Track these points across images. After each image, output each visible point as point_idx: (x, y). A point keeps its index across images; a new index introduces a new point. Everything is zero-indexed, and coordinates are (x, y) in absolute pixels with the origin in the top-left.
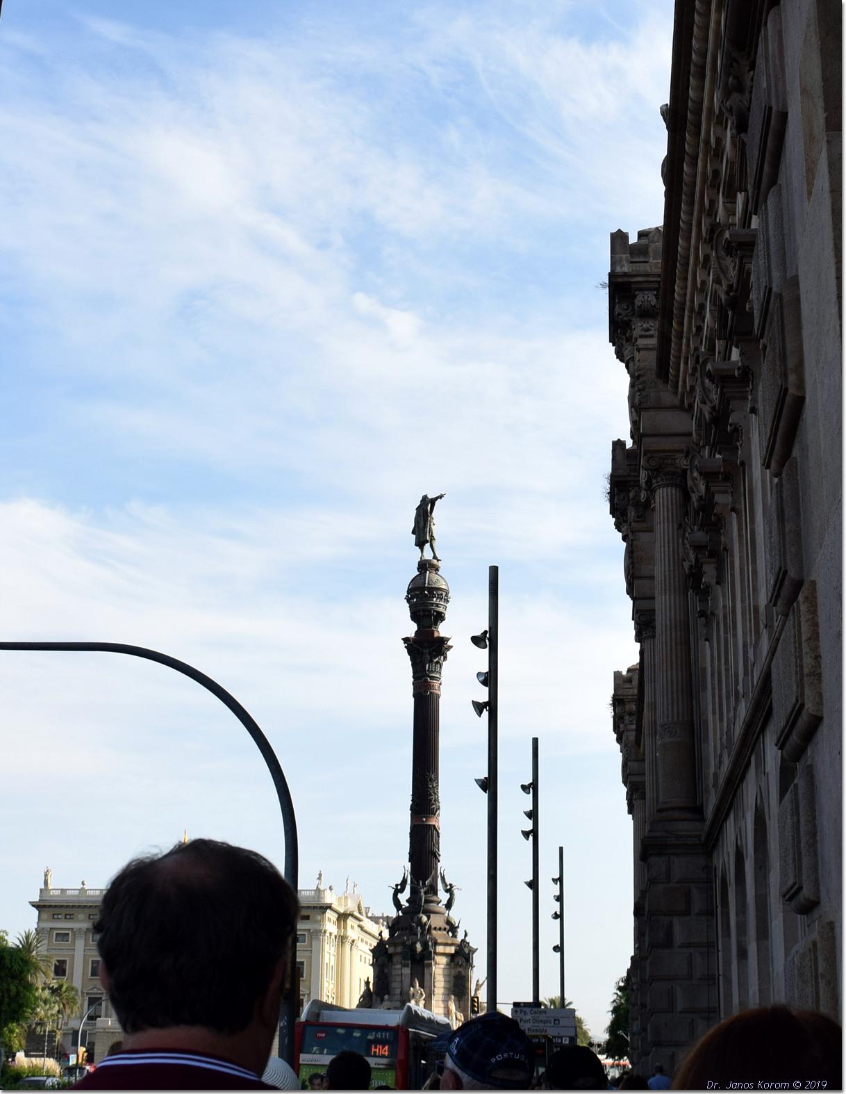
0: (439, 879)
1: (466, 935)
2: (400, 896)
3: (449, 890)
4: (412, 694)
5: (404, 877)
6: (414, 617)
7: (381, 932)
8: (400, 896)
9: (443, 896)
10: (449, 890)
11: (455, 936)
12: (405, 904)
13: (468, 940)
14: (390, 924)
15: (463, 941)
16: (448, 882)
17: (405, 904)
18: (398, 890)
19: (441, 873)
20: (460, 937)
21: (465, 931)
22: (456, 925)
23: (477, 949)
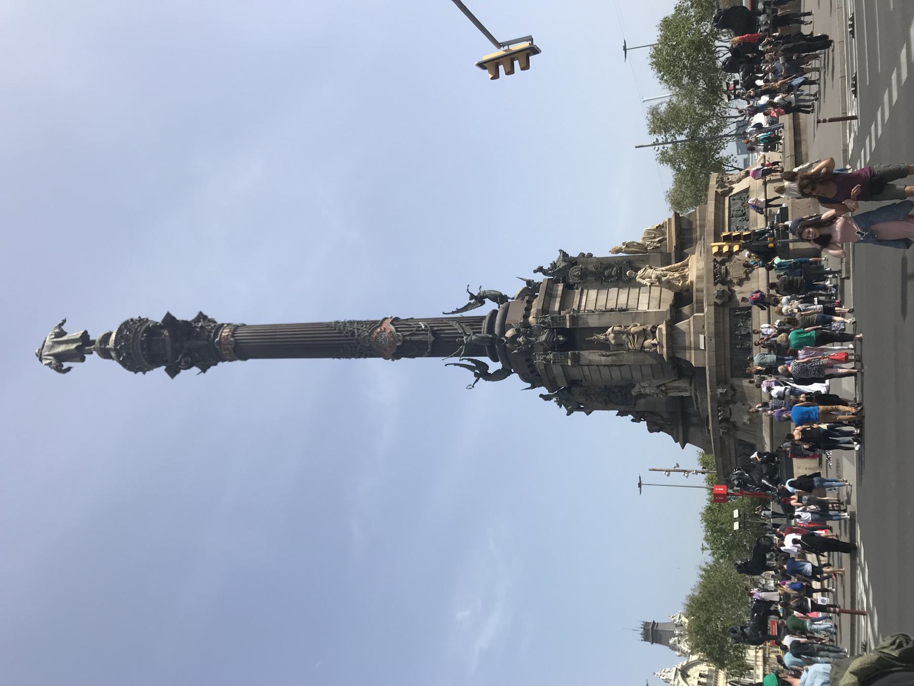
0: (466, 314)
1: (540, 269)
3: (479, 300)
4: (243, 362)
7: (541, 396)
9: (490, 306)
10: (479, 300)
12: (498, 366)
14: (529, 385)
16: (466, 300)
17: (498, 366)
18: (482, 372)
19: (453, 312)
20: (540, 278)
21: (535, 272)
23: (561, 251)
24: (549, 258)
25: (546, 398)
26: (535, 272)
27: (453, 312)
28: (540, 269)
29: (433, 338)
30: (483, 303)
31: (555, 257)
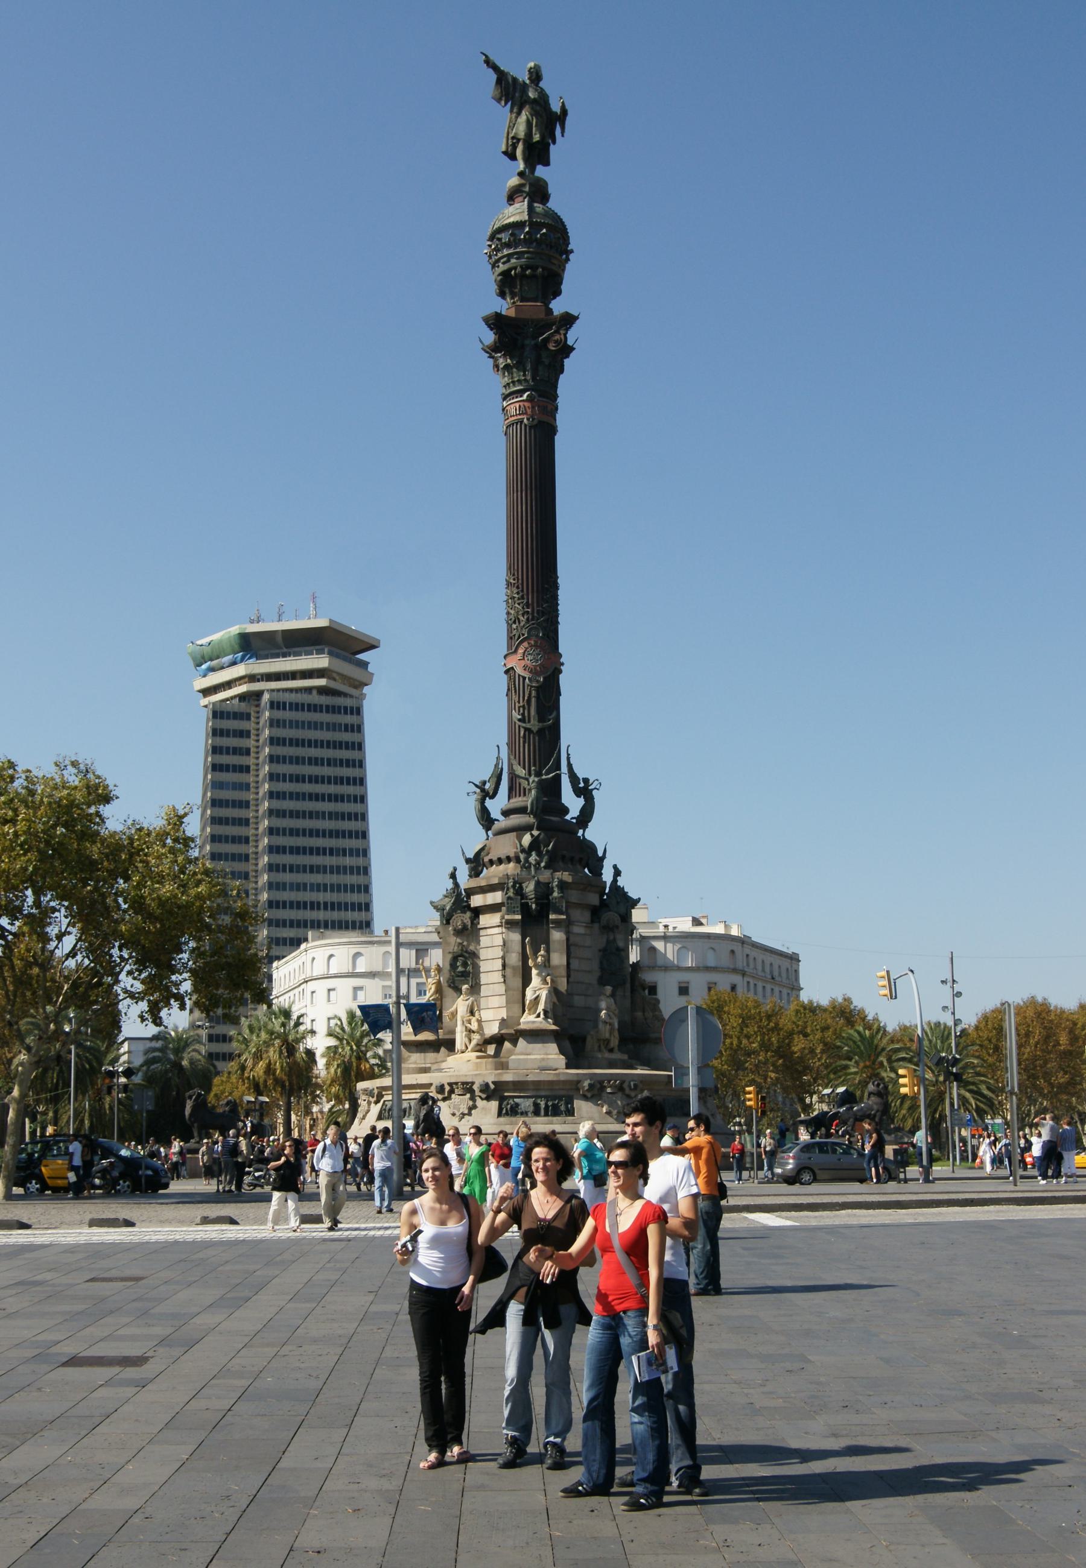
1: (617, 873)
2: (488, 803)
5: (496, 765)
6: (507, 284)
7: (455, 869)
8: (488, 803)
9: (573, 804)
10: (584, 790)
11: (597, 871)
13: (621, 882)
15: (615, 881)
16: (581, 775)
18: (486, 793)
19: (568, 759)
21: (615, 867)
22: (600, 854)
24: (630, 885)
25: (453, 876)
26: (615, 867)
27: (568, 759)
28: (617, 873)
29: (535, 729)
30: (578, 796)
31: (633, 895)
